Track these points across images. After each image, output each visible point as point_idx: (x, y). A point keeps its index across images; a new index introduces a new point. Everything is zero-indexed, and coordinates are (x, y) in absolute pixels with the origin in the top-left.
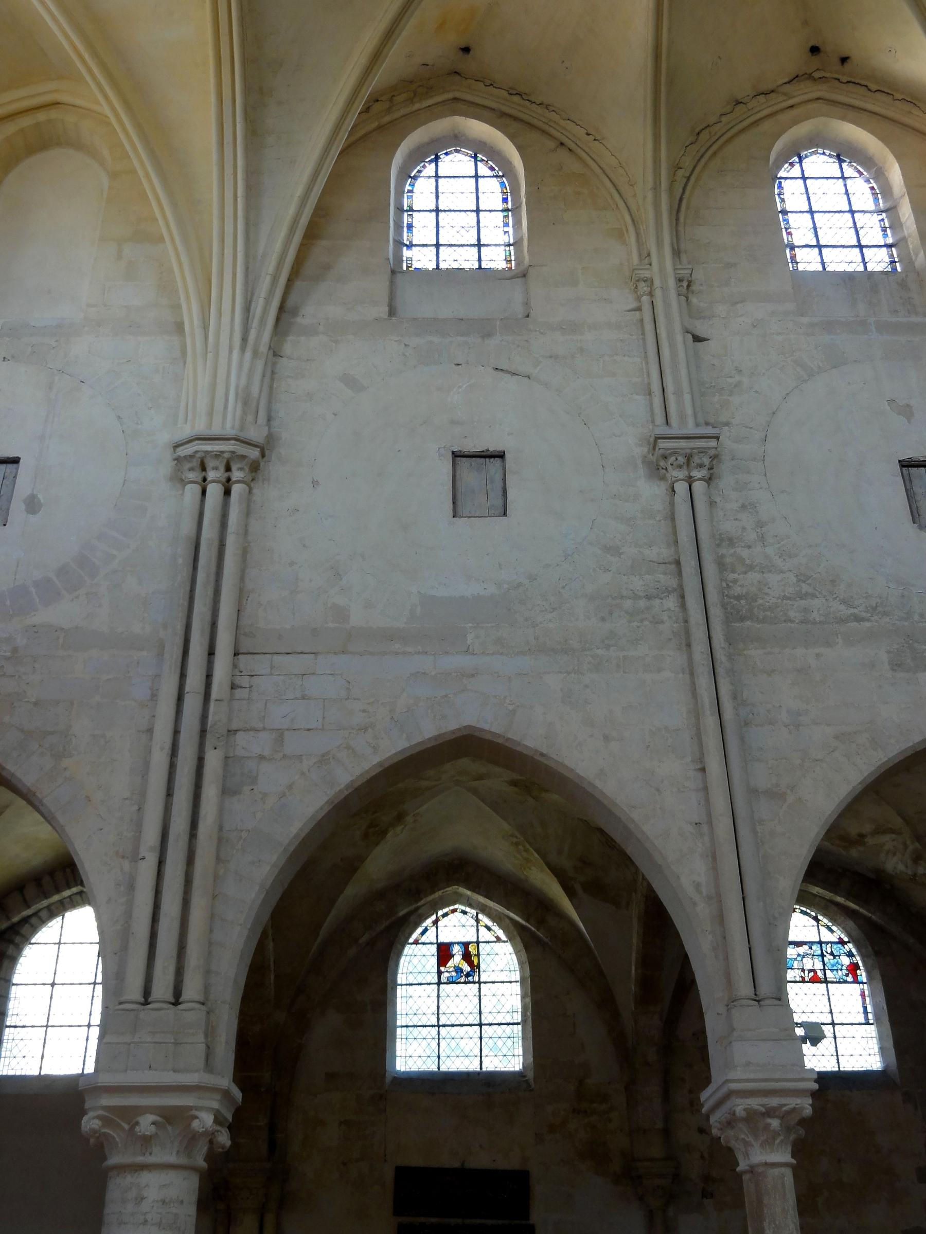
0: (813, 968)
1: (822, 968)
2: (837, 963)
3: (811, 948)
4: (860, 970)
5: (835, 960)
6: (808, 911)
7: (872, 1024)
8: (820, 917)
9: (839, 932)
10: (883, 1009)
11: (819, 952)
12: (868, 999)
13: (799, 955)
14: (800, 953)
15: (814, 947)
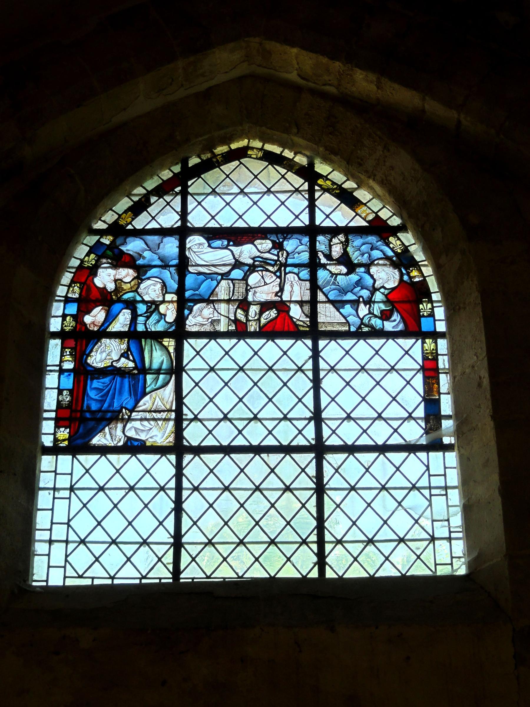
0: (277, 299)
1: (307, 297)
2: (358, 283)
3: (278, 246)
4: (431, 301)
5: (354, 277)
6: (288, 154)
7: (449, 448)
8: (322, 168)
9: (376, 205)
10: (480, 385)
11: (305, 257)
12: (444, 381)
13: (237, 264)
14: (242, 260)
15: (290, 245)
